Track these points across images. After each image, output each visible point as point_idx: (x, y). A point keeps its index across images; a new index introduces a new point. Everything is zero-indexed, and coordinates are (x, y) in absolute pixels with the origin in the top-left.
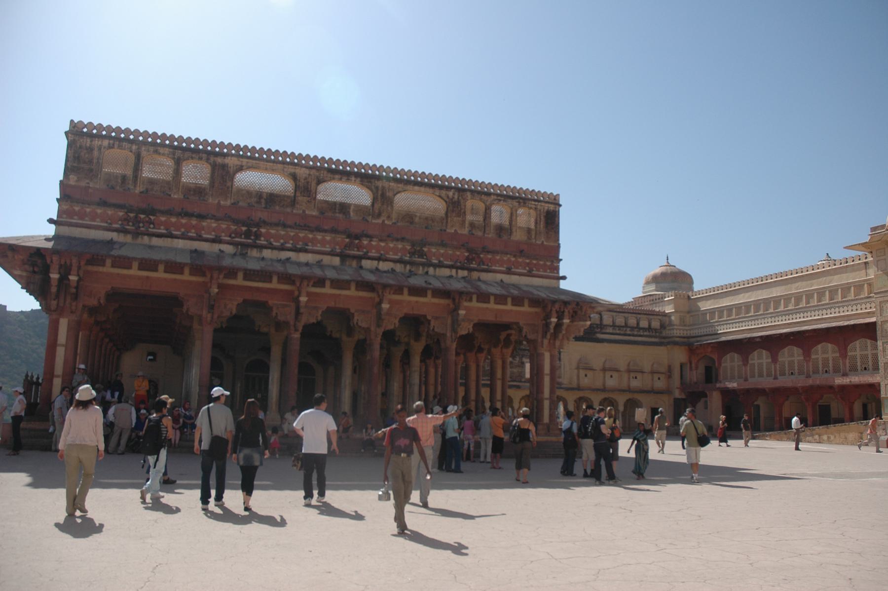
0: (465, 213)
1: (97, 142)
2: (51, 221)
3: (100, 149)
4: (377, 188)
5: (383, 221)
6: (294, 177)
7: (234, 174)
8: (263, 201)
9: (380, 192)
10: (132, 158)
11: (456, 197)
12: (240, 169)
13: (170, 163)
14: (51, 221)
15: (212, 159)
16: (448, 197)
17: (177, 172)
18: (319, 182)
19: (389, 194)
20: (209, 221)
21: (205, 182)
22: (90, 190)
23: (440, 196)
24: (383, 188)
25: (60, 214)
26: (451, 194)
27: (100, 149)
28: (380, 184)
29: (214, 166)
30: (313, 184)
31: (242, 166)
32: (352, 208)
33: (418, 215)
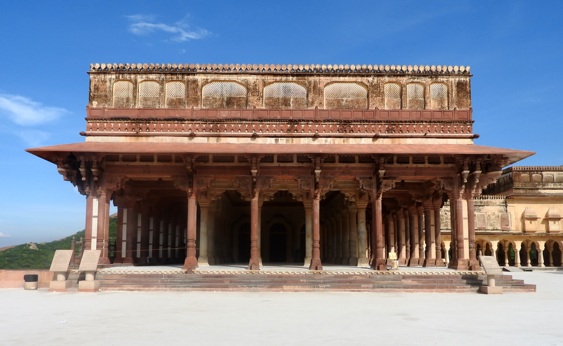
0: (383, 92)
1: (108, 77)
3: (110, 81)
4: (310, 83)
7: (202, 86)
8: (225, 103)
9: (312, 86)
10: (131, 85)
11: (376, 81)
12: (206, 82)
15: (186, 77)
16: (369, 82)
17: (162, 90)
18: (265, 84)
19: (321, 86)
20: (187, 122)
22: (106, 110)
24: (315, 82)
26: (370, 79)
27: (110, 81)
28: (312, 79)
29: (188, 83)
30: (261, 86)
31: (207, 79)
32: (292, 100)
33: (345, 99)
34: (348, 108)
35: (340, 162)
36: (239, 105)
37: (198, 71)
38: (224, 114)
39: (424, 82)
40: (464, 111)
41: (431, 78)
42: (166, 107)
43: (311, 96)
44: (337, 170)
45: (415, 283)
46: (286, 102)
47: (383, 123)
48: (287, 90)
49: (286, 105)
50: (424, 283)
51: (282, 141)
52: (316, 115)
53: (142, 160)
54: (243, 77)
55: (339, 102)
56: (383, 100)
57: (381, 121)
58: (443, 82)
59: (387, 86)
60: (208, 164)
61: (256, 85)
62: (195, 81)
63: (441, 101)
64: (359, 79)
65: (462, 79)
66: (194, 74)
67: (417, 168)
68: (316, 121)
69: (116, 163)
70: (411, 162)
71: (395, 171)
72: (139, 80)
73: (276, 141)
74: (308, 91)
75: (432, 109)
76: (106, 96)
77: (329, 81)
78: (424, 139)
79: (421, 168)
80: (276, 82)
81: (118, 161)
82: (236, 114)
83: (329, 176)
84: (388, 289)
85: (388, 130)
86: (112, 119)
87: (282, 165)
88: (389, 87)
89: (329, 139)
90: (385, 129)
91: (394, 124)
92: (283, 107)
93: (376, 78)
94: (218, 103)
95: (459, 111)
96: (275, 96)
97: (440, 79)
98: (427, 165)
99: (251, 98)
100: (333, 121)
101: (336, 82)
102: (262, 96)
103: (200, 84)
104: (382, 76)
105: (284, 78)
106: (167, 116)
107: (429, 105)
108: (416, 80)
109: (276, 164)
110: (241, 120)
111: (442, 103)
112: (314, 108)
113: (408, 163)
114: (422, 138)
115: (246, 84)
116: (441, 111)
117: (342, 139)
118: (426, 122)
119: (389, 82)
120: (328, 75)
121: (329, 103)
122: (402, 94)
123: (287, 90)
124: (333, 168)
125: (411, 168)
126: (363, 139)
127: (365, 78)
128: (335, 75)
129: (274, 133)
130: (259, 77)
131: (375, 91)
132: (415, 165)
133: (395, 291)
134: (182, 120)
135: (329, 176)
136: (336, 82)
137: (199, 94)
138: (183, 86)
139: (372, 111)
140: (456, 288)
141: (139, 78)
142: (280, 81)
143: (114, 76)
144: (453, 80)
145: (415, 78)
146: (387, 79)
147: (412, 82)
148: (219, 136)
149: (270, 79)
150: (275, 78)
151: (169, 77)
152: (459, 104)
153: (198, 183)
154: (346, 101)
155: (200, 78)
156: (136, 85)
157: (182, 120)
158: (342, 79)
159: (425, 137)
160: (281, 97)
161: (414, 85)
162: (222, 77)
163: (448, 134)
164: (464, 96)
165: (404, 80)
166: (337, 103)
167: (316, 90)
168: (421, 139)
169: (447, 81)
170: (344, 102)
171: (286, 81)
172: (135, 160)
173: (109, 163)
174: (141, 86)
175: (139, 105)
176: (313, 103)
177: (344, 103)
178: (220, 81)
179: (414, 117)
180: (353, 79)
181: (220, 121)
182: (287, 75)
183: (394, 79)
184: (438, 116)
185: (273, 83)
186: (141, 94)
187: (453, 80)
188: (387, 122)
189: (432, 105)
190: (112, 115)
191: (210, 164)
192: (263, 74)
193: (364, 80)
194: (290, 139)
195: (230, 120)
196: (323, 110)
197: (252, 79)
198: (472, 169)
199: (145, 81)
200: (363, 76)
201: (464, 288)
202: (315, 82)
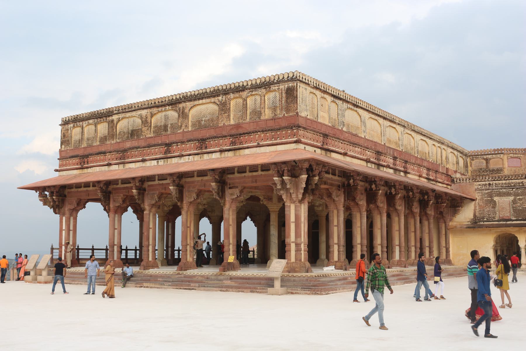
0: (229, 109)
1: (70, 126)
2: (56, 171)
5: (183, 130)
6: (141, 117)
7: (117, 124)
8: (130, 135)
9: (181, 111)
11: (224, 99)
13: (93, 127)
14: (56, 171)
17: (96, 131)
18: (152, 115)
21: (106, 132)
23: (214, 102)
25: (60, 166)
26: (220, 98)
30: (149, 117)
33: (203, 119)
34: (205, 127)
35: (198, 176)
36: (137, 136)
37: (115, 112)
38: (128, 145)
39: (260, 93)
40: (291, 116)
41: (265, 88)
42: (98, 143)
43: (180, 121)
44: (196, 183)
45: (233, 284)
46: (165, 127)
47: (228, 138)
48: (166, 118)
49: (166, 131)
50: (240, 284)
51: (161, 162)
52: (183, 137)
53: (85, 187)
54: (139, 112)
55: (199, 122)
56: (229, 116)
57: (226, 136)
58: (275, 91)
59: (233, 103)
60: (118, 186)
61: (147, 118)
62: (112, 121)
63: (274, 109)
64: (213, 100)
65: (291, 85)
66: (112, 115)
67: (252, 177)
68: (183, 142)
69: (73, 190)
70: (247, 171)
71: (237, 181)
72: (84, 125)
73: (158, 162)
74: (179, 116)
75: (267, 117)
76: (68, 141)
77: (192, 105)
78: (258, 148)
79: (256, 176)
80: (159, 112)
81: (73, 188)
82: (135, 143)
83: (191, 189)
84: (208, 288)
85: (233, 143)
86: (70, 157)
87: (161, 182)
88: (235, 102)
89: (191, 157)
90: (230, 142)
91: (237, 137)
92: (164, 133)
93: (224, 96)
94: (126, 135)
95: (287, 117)
96: (159, 124)
97: (273, 88)
98: (260, 173)
99: (143, 129)
100: (193, 141)
101: (198, 105)
102: (151, 126)
103: (115, 122)
104: (228, 94)
105: (163, 108)
106: (97, 151)
107: (263, 114)
108: (254, 93)
109: (157, 182)
110: (137, 148)
111: (275, 111)
112: (181, 131)
113: (245, 172)
114: (257, 147)
115: (141, 117)
116: (273, 119)
117: (199, 156)
118: (259, 131)
119: (234, 98)
120: (191, 101)
121: (193, 125)
122: (245, 106)
123: (166, 118)
124: (193, 182)
125: (249, 177)
126: (214, 154)
127: (216, 98)
128: (195, 100)
129: (154, 157)
130: (148, 111)
131: (224, 108)
132: (250, 174)
133: (213, 290)
134: (104, 153)
135: (191, 189)
136: (198, 105)
137: (115, 131)
138: (106, 125)
139: (221, 127)
140: (257, 289)
141: (85, 124)
142: (162, 111)
143: (72, 125)
144: (283, 87)
145: (253, 91)
146: (232, 95)
147: (252, 95)
148: (124, 163)
149: (155, 110)
150: (158, 109)
151: (99, 120)
152: (288, 110)
153: (114, 201)
154: (205, 121)
155: (115, 117)
156: (82, 129)
157: (104, 153)
158: (201, 102)
159: (259, 146)
160: (163, 124)
161: (253, 97)
162: (128, 115)
163: (278, 141)
164: (292, 101)
165: (244, 94)
166: (198, 124)
167: (183, 115)
168: (256, 148)
169: (278, 89)
170: (203, 122)
171: (165, 110)
172: (81, 187)
173: (70, 190)
174: (86, 130)
175: (84, 145)
176: (181, 126)
177: (203, 122)
178: (128, 118)
179: (251, 129)
180: (208, 100)
181: (125, 151)
182: (164, 106)
183: (237, 95)
184: (271, 124)
185: (157, 113)
186: (86, 136)
187: (283, 87)
188: (231, 136)
189: (267, 114)
190: (72, 154)
191: (120, 186)
192: (150, 108)
193: (216, 99)
194: (166, 160)
195: (133, 148)
196: (188, 132)
197: (144, 112)
198: (281, 175)
199: (88, 125)
200: (214, 97)
201: (263, 289)
202: (183, 107)
